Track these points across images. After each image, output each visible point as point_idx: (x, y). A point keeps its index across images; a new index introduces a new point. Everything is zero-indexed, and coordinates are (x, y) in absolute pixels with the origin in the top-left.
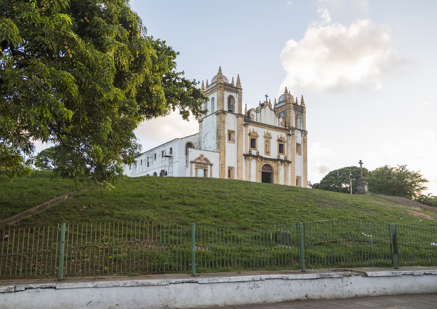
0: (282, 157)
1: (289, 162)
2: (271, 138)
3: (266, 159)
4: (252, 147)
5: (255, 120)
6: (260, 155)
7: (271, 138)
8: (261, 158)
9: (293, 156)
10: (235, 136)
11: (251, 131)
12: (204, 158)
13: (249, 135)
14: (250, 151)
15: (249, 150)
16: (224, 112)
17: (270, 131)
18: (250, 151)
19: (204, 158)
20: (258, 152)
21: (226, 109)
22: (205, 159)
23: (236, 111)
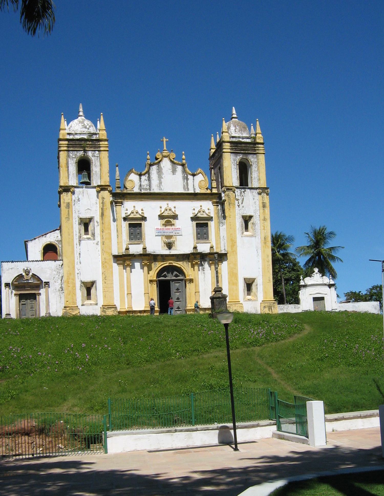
0: (204, 248)
1: (222, 257)
2: (175, 217)
3: (164, 257)
4: (131, 239)
5: (136, 190)
6: (150, 250)
7: (175, 217)
8: (155, 258)
9: (233, 242)
10: (95, 227)
11: (129, 212)
12: (31, 274)
13: (125, 219)
14: (127, 249)
15: (124, 247)
16: (67, 189)
17: (172, 204)
18: (127, 249)
19: (31, 274)
20: (145, 249)
21: (73, 181)
22: (34, 275)
23: (96, 181)
